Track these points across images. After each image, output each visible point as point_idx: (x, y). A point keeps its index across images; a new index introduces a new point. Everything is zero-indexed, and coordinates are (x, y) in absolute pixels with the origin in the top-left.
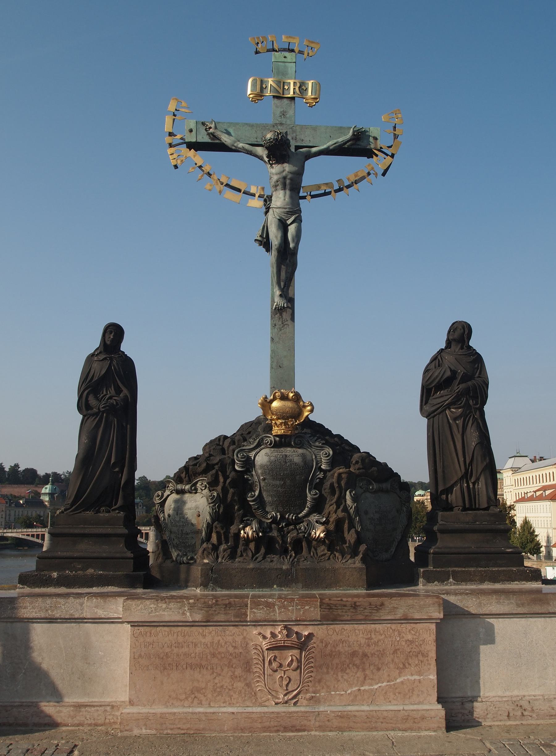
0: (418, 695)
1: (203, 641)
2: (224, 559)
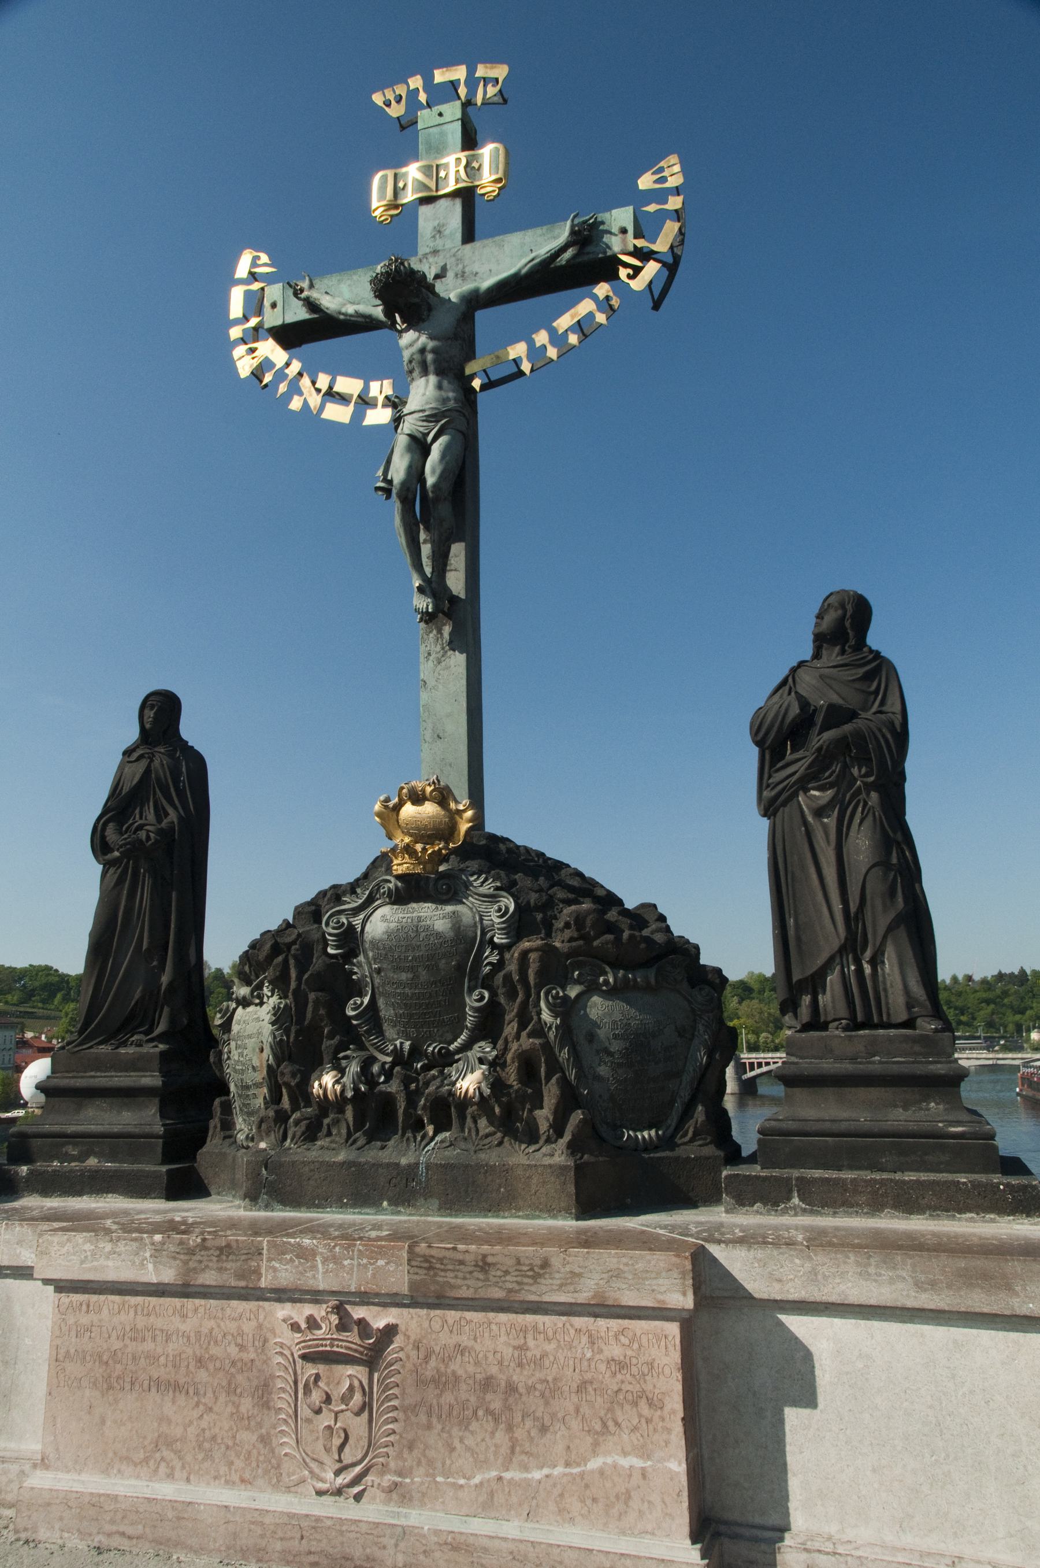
1: (183, 1327)
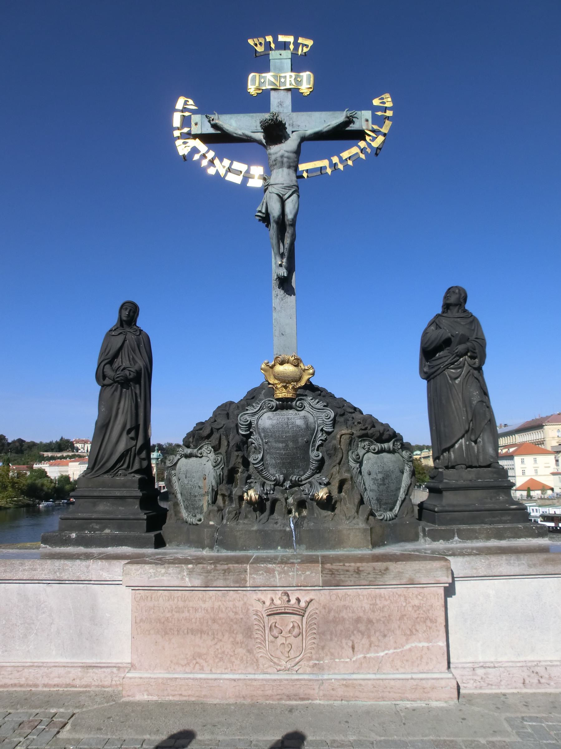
0: (427, 663)
1: (203, 606)
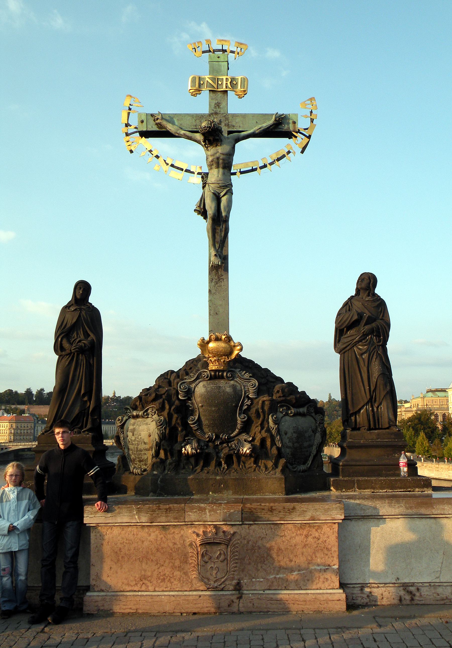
1: (149, 538)
2: (170, 471)
